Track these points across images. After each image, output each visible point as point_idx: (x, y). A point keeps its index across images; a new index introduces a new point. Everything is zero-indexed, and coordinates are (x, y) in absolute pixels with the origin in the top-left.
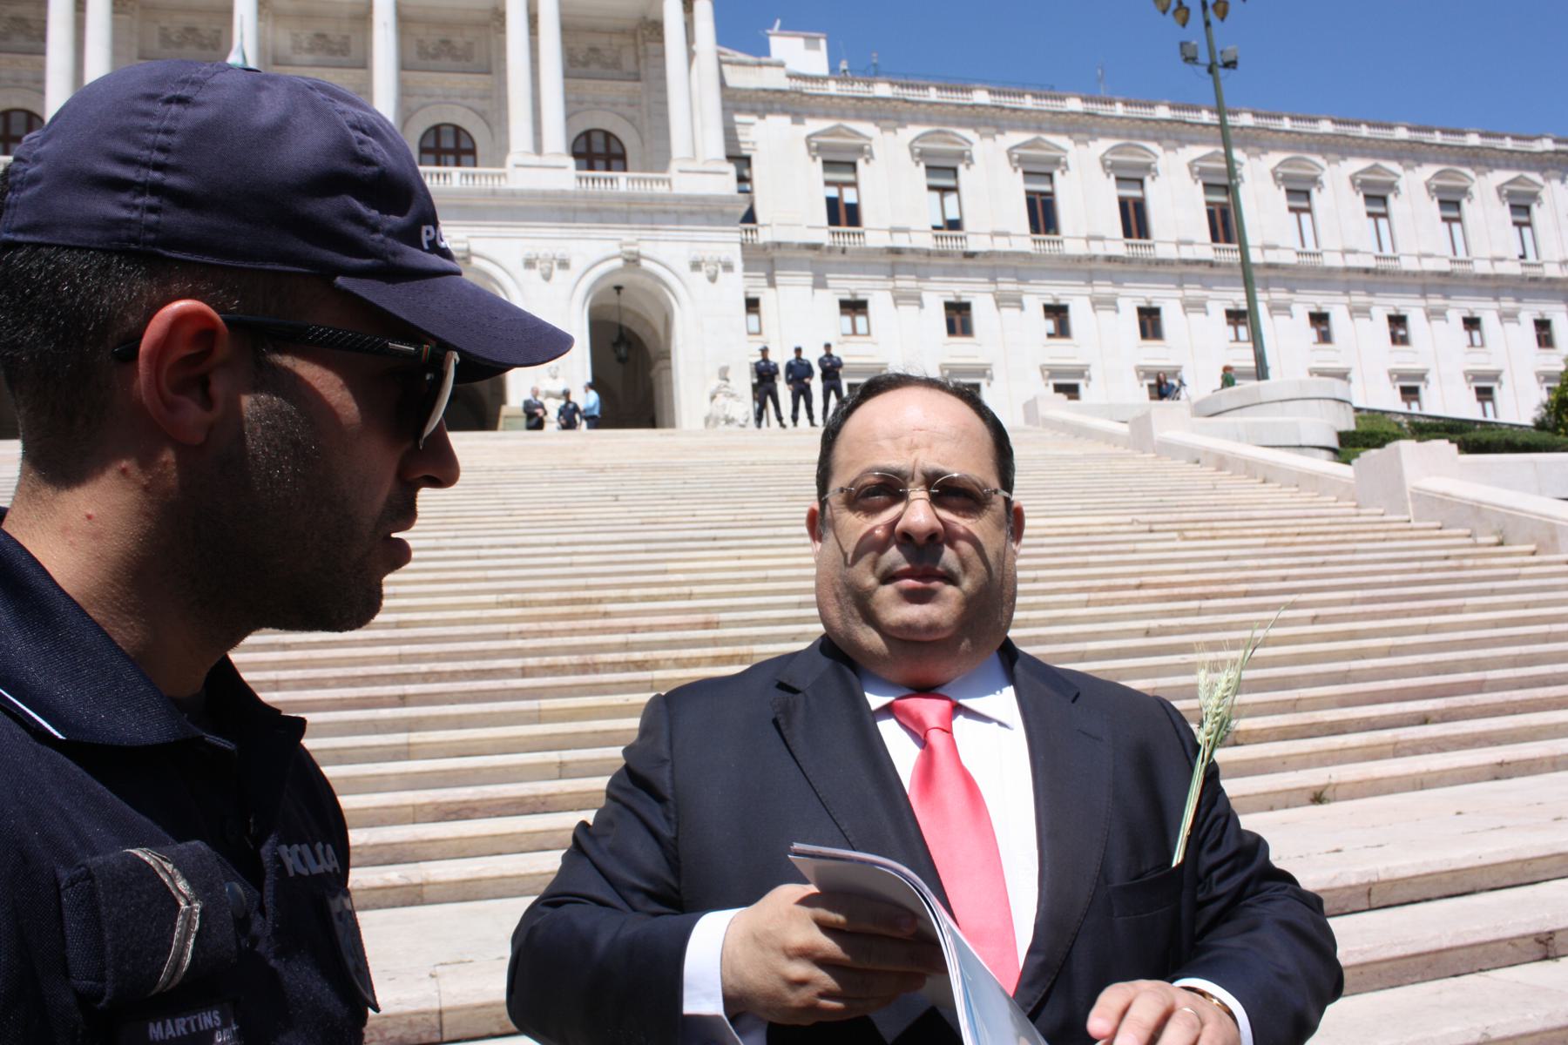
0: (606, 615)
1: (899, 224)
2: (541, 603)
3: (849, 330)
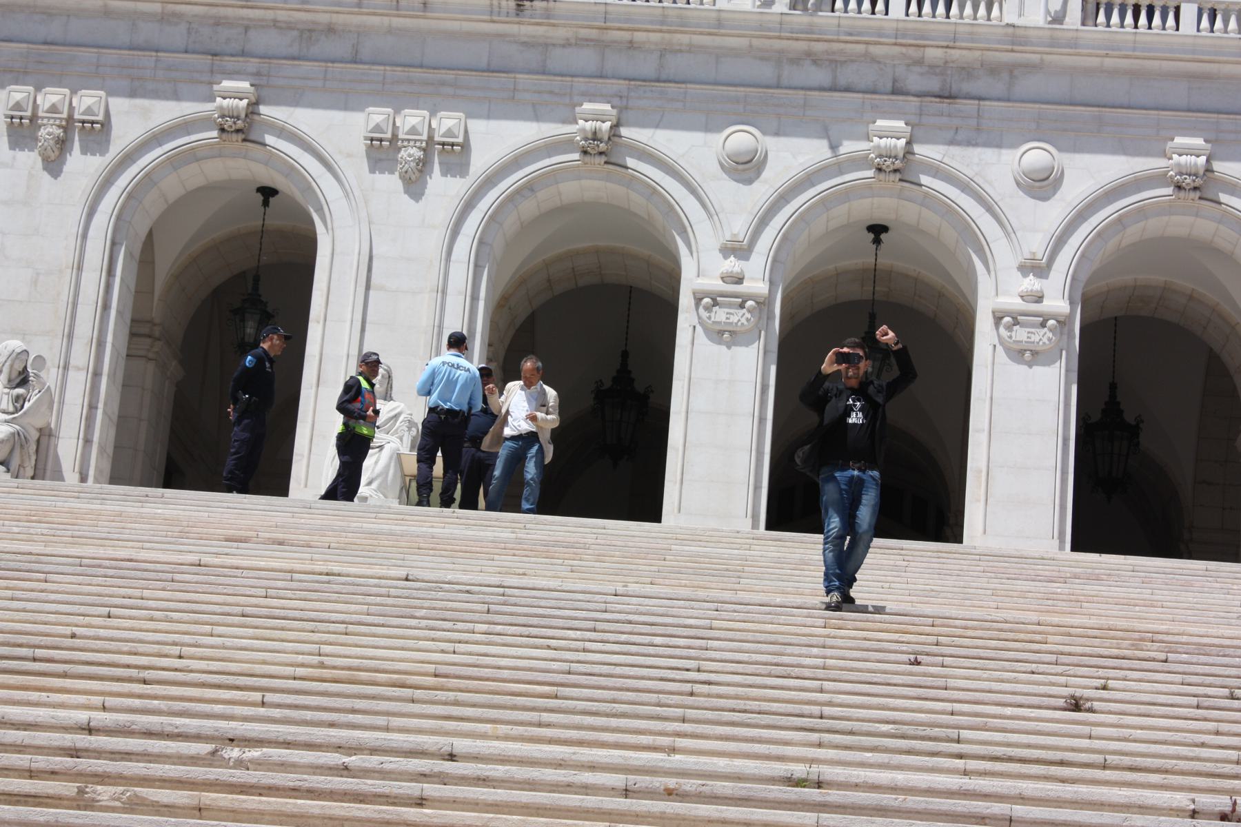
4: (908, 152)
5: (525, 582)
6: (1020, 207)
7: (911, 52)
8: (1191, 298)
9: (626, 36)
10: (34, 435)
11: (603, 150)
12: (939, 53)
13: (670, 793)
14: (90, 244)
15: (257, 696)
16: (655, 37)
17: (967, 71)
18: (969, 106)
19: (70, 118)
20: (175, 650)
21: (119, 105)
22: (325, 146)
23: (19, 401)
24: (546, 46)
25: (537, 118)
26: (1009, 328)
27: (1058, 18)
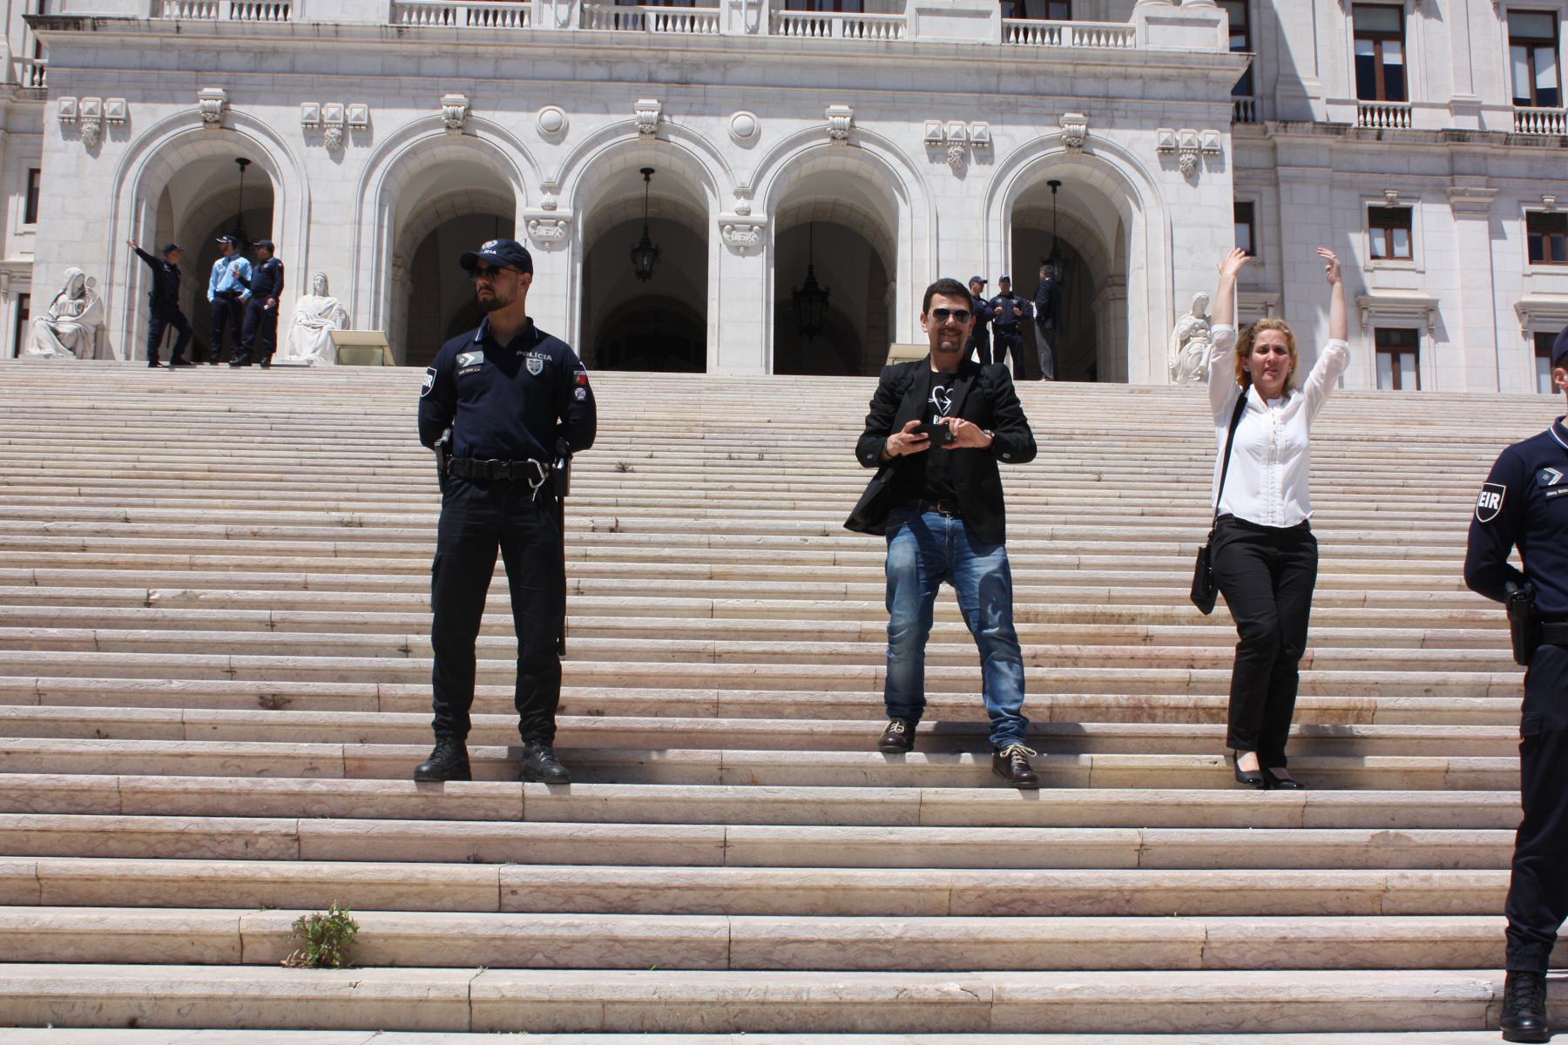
0: (1147, 639)
1: (1465, 94)
2: (1051, 618)
3: (1381, 251)
4: (660, 120)
5: (343, 409)
6: (734, 154)
7: (660, 54)
8: (851, 209)
9: (472, 49)
10: (93, 330)
11: (461, 125)
12: (677, 55)
13: (255, 535)
14: (121, 202)
15: (75, 490)
16: (492, 49)
17: (696, 66)
18: (699, 89)
19: (103, 118)
20: (39, 463)
21: (135, 107)
22: (275, 128)
23: (80, 307)
24: (420, 58)
25: (416, 106)
26: (729, 232)
27: (754, 30)
